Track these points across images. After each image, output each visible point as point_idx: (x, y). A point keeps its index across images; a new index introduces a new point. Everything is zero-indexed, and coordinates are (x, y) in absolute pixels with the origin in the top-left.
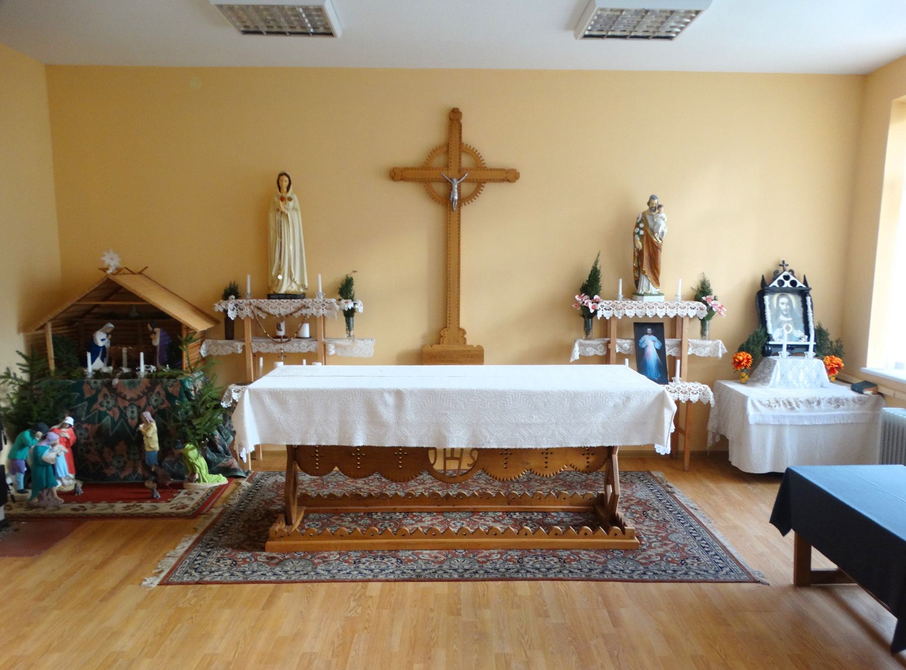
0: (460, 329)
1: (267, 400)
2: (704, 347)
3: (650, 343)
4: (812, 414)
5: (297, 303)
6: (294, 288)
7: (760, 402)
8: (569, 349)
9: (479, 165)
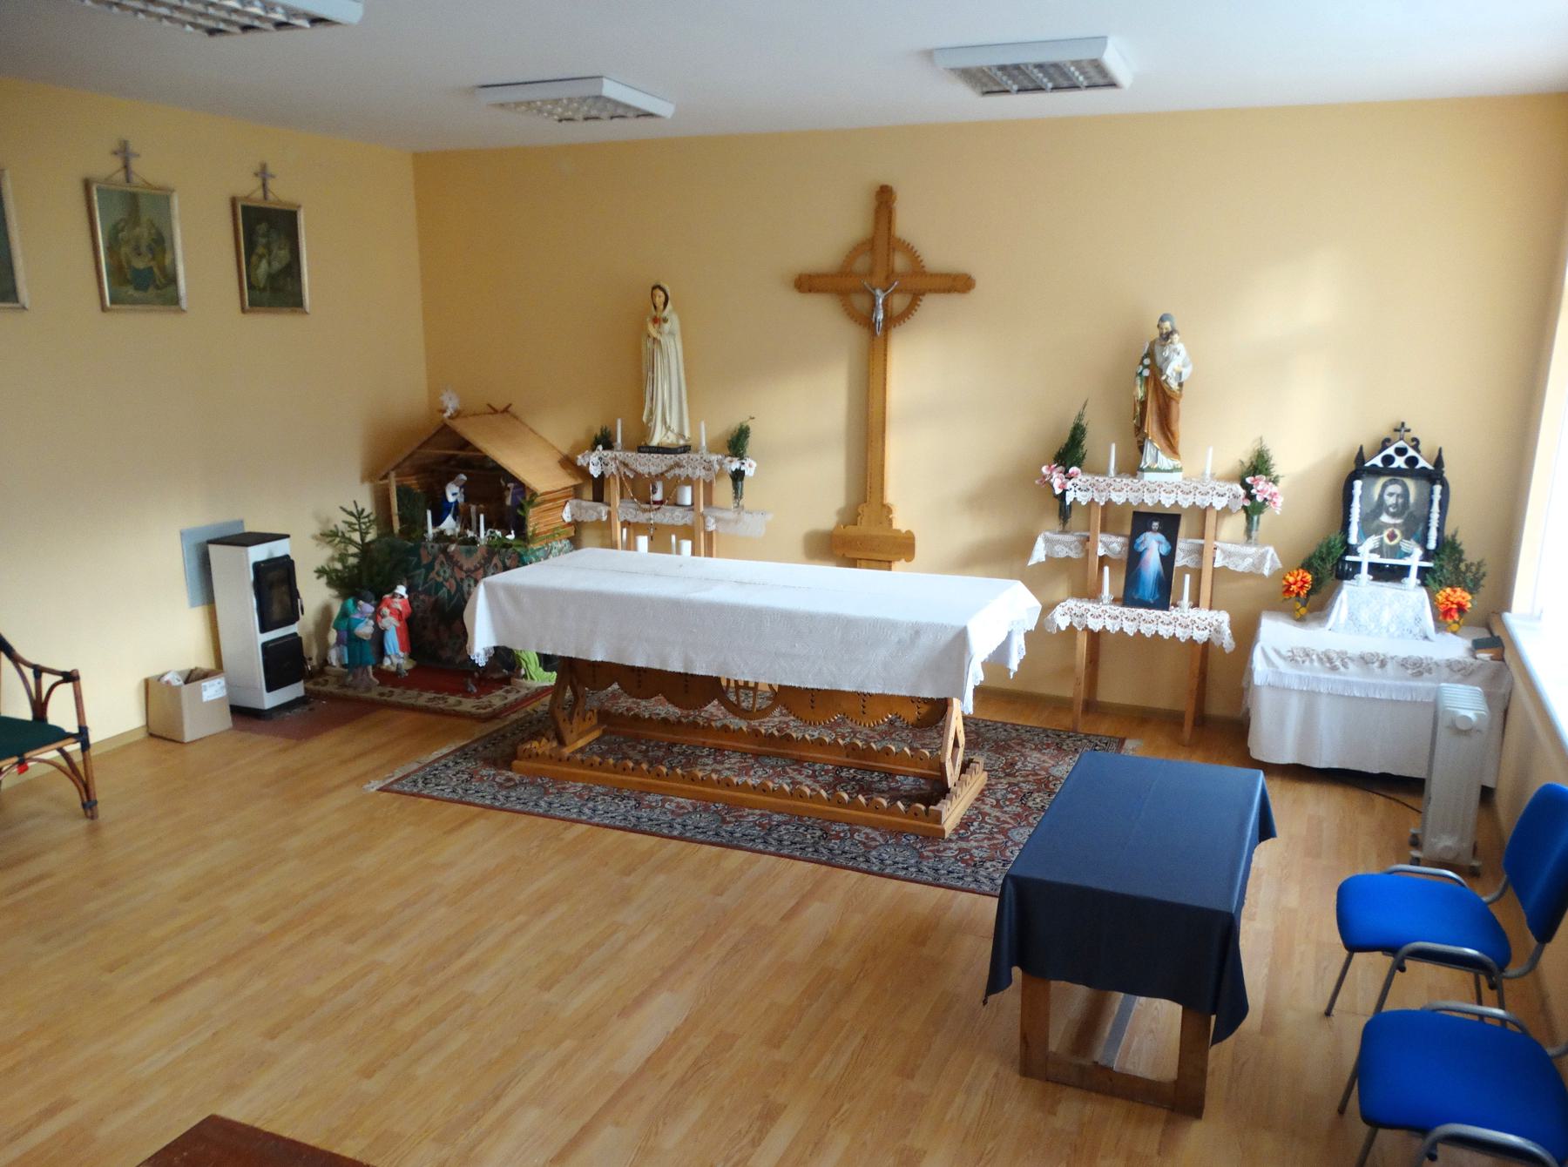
0: (884, 506)
1: (502, 595)
2: (1244, 557)
3: (1153, 545)
4: (1368, 680)
5: (670, 459)
6: (670, 439)
7: (1278, 652)
8: (1028, 546)
9: (917, 267)
